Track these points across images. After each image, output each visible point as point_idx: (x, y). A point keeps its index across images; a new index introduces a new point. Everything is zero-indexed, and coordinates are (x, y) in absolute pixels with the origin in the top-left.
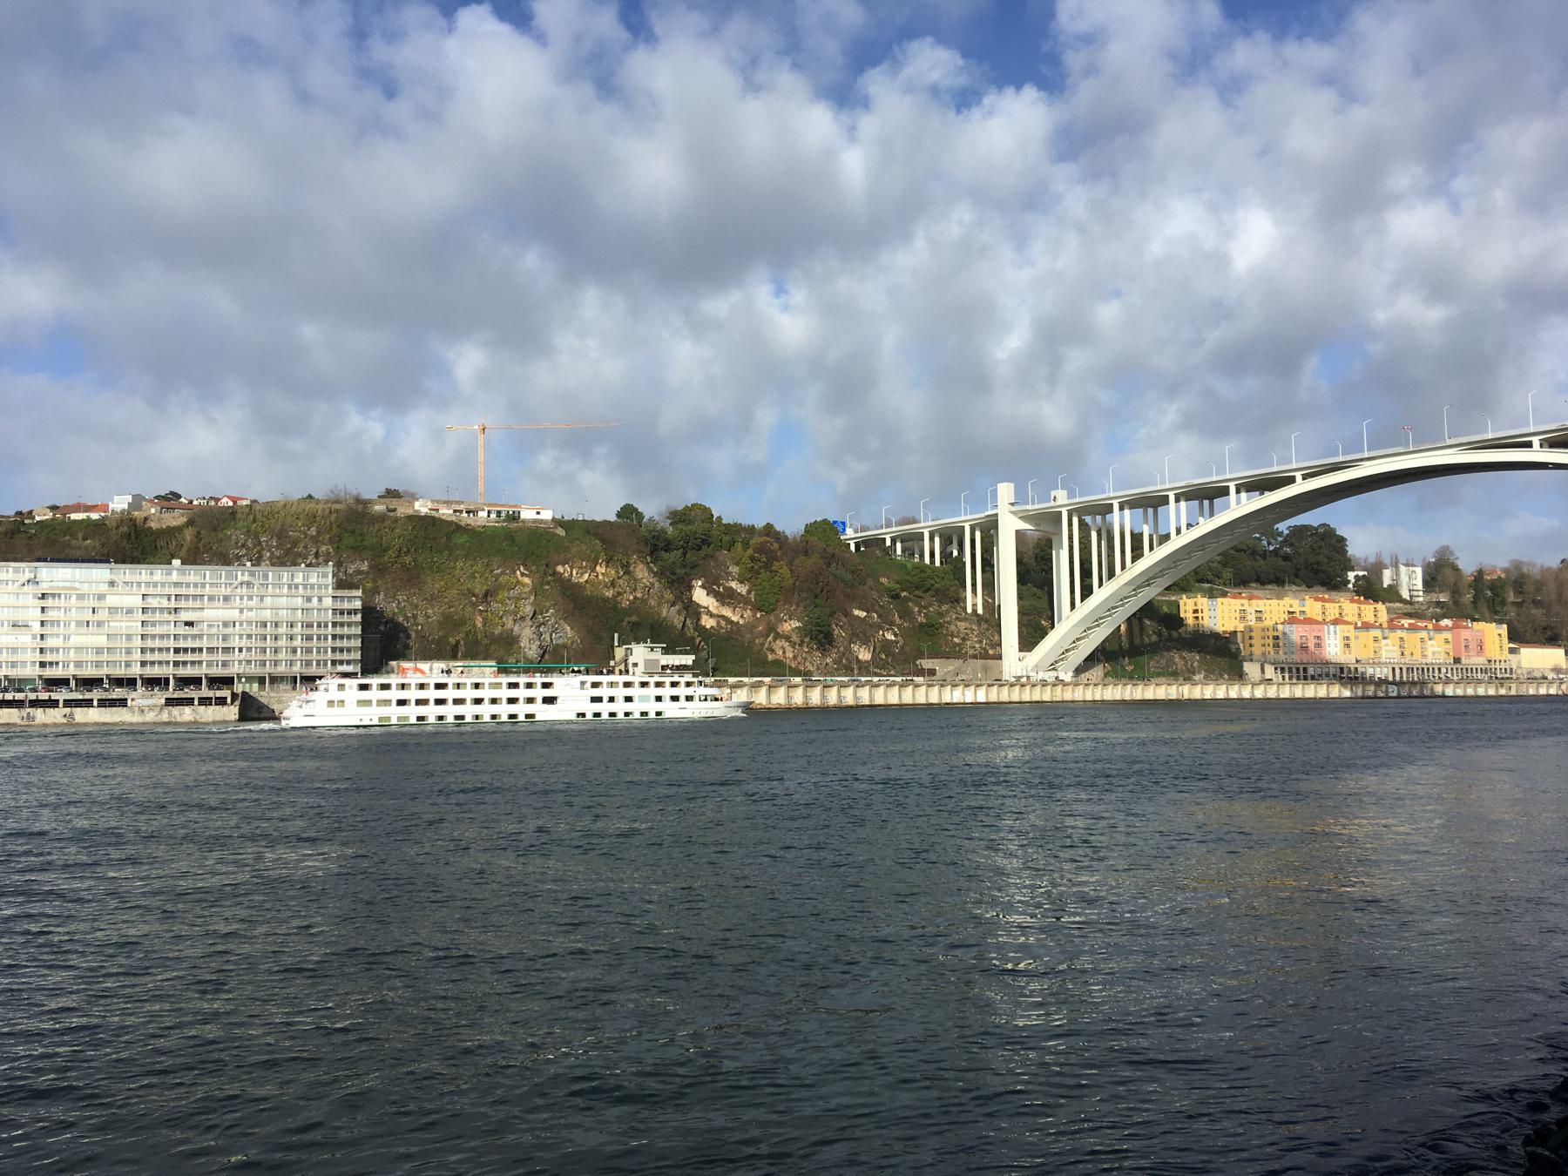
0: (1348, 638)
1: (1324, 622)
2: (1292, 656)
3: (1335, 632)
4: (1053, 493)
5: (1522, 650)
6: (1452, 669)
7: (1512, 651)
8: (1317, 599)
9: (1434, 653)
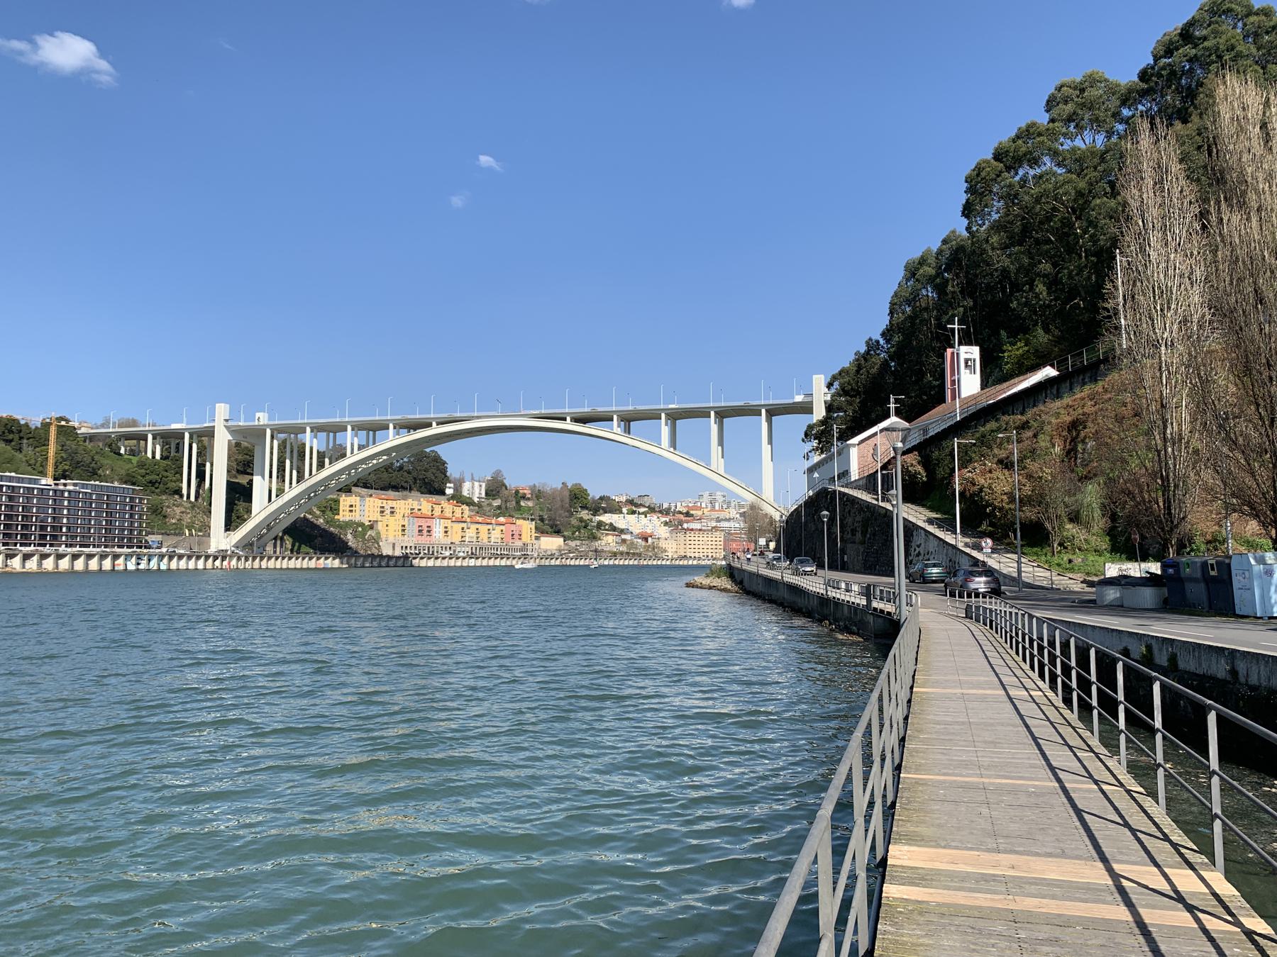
0: (446, 527)
1: (432, 517)
4: (258, 415)
5: (542, 538)
7: (537, 538)
8: (428, 502)
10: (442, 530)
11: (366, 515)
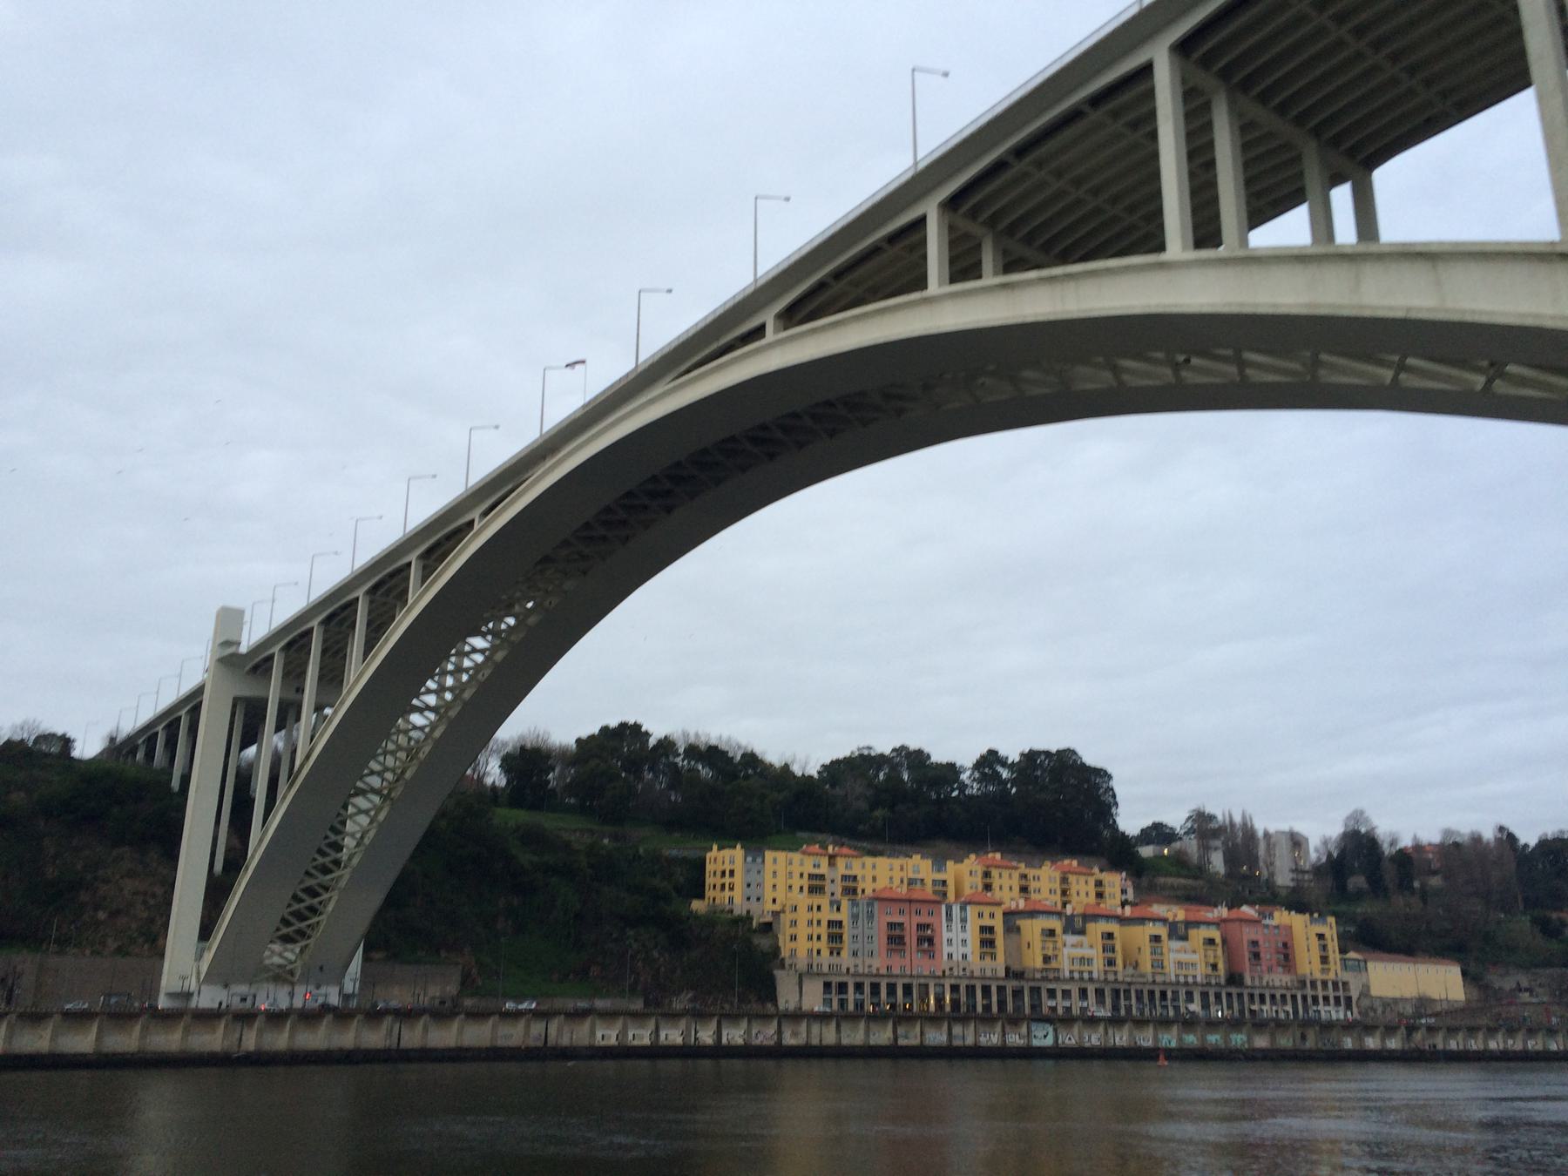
0: (991, 929)
2: (868, 961)
3: (964, 920)
6: (1218, 997)
9: (1180, 964)
10: (972, 936)
11: (768, 895)
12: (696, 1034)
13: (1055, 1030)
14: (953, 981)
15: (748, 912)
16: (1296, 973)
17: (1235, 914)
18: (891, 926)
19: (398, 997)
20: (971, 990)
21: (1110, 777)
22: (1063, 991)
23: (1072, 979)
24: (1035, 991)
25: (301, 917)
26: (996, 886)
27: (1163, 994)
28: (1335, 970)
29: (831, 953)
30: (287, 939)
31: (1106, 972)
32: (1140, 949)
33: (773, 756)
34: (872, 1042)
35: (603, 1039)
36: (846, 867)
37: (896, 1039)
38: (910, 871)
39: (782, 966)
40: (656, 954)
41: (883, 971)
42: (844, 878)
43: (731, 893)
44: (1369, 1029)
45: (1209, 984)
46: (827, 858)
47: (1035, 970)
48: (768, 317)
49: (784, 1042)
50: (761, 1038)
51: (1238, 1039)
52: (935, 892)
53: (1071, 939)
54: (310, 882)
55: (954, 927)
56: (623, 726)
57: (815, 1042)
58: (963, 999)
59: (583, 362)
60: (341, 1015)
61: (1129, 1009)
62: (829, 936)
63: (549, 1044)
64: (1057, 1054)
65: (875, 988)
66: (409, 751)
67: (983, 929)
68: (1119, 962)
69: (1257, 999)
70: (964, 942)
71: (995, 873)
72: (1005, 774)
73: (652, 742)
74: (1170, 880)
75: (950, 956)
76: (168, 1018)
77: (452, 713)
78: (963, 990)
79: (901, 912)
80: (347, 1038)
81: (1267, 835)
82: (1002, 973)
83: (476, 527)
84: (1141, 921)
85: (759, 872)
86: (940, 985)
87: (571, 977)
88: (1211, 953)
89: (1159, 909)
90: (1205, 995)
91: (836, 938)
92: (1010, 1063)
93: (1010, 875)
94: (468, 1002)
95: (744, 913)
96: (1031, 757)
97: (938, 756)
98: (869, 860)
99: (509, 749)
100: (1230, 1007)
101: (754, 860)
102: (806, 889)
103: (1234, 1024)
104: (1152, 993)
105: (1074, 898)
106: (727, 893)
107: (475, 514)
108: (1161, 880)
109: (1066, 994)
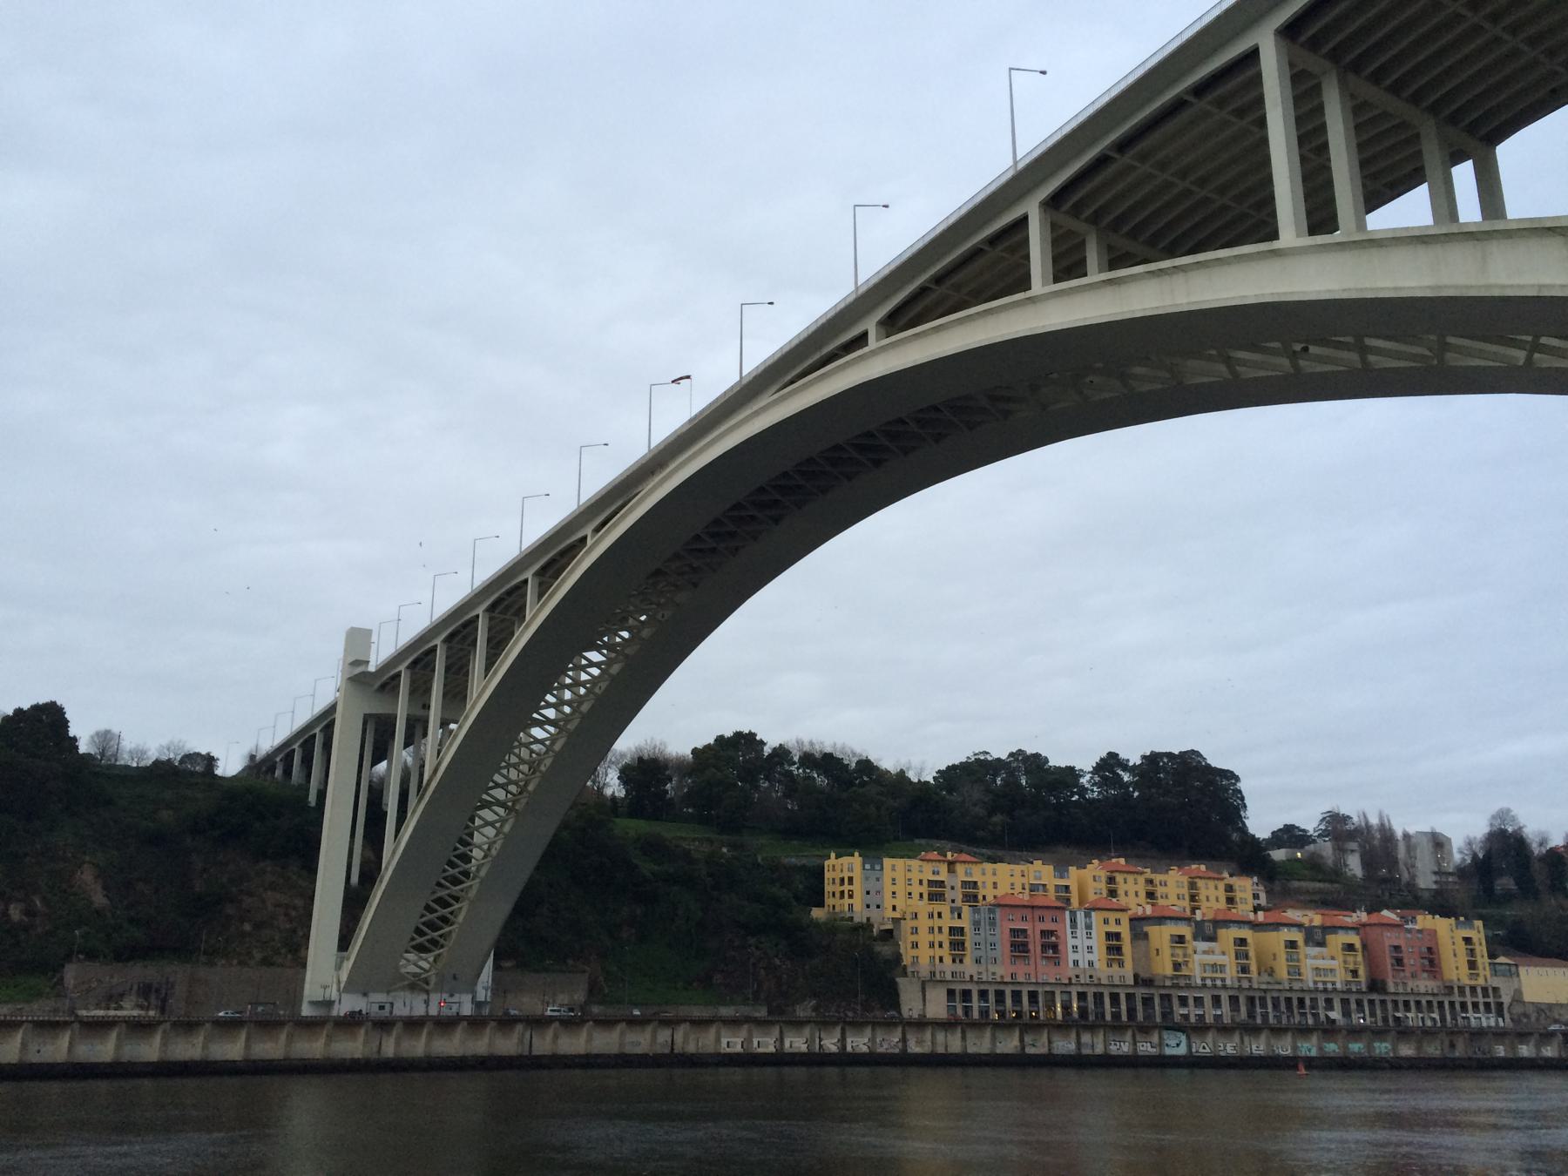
0: (1117, 936)
2: (992, 968)
5: (1522, 970)
6: (1359, 1003)
10: (1098, 942)
11: (888, 902)
12: (820, 1042)
13: (1188, 1038)
14: (1080, 989)
15: (868, 919)
16: (1442, 979)
17: (1375, 918)
18: (1014, 932)
19: (525, 1003)
20: (1099, 997)
21: (1237, 779)
22: (1196, 999)
23: (1204, 986)
24: (1166, 998)
25: (432, 926)
26: (1121, 892)
27: (1301, 1001)
28: (1485, 976)
29: (954, 961)
30: (421, 949)
31: (1239, 979)
32: (1274, 955)
33: (888, 763)
34: (998, 1051)
35: (728, 1047)
36: (966, 872)
37: (1023, 1048)
38: (1032, 875)
39: (905, 974)
40: (777, 962)
41: (1008, 979)
42: (964, 884)
43: (851, 901)
44: (1523, 1036)
45: (1349, 991)
46: (946, 864)
47: (1165, 977)
48: (870, 325)
49: (909, 1051)
50: (885, 1046)
51: (1382, 1048)
52: (1058, 898)
53: (1202, 946)
54: (442, 893)
55: (1079, 935)
56: (738, 735)
57: (941, 1050)
58: (1091, 1006)
59: (688, 377)
60: (476, 1023)
61: (1265, 1016)
62: (950, 943)
63: (676, 1051)
64: (1192, 1063)
65: (1000, 995)
66: (531, 764)
67: (1109, 936)
68: (1254, 968)
69: (1401, 1006)
70: (1090, 948)
71: (1119, 878)
72: (1126, 777)
73: (767, 750)
74: (1304, 884)
75: (1076, 963)
76: (311, 1025)
77: (571, 726)
78: (1090, 999)
79: (1024, 919)
80: (481, 1045)
81: (1406, 836)
82: (1132, 983)
83: (589, 542)
84: (1276, 926)
85: (878, 879)
86: (1067, 992)
87: (695, 984)
88: (1350, 959)
89: (1293, 915)
90: (1345, 1002)
91: (958, 945)
92: (1144, 1072)
93: (1135, 880)
94: (596, 1009)
95: (865, 920)
96: (1153, 759)
97: (1057, 760)
98: (989, 866)
99: (627, 760)
100: (1373, 1014)
101: (873, 868)
102: (926, 896)
103: (1378, 1033)
104: (1288, 1000)
105: (1204, 904)
106: (847, 901)
107: (588, 530)
108: (1296, 884)
109: (1199, 1002)
